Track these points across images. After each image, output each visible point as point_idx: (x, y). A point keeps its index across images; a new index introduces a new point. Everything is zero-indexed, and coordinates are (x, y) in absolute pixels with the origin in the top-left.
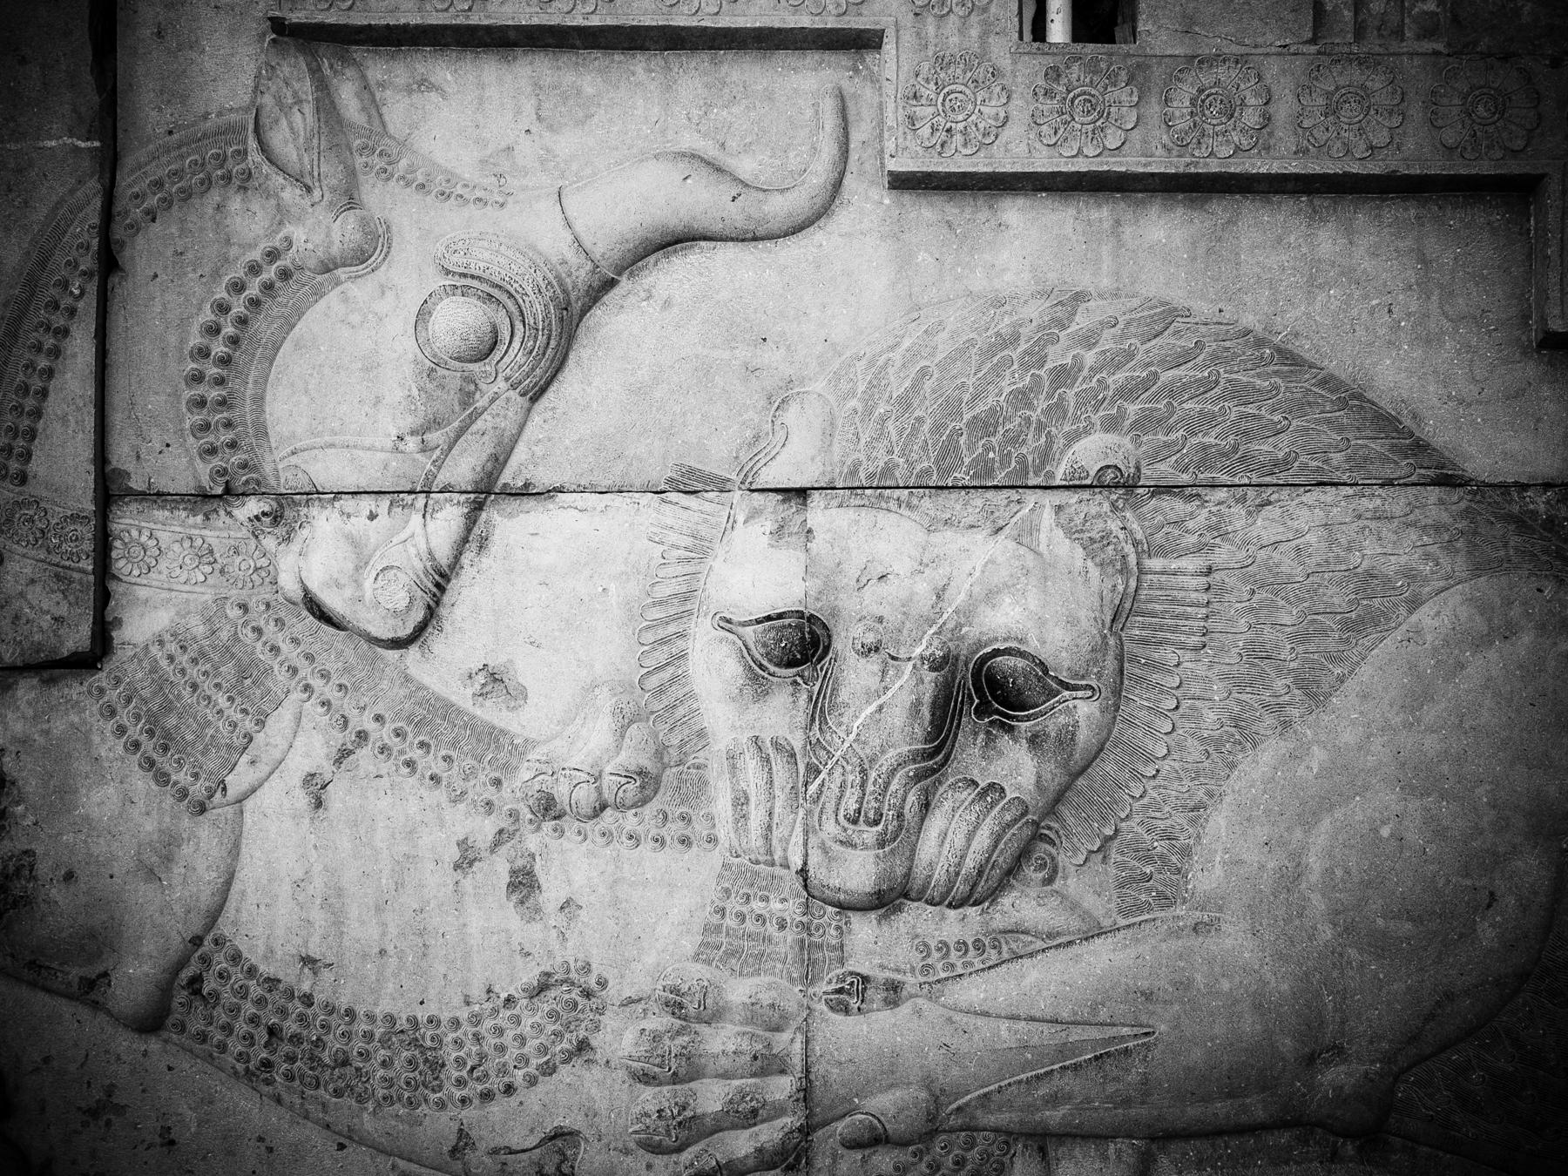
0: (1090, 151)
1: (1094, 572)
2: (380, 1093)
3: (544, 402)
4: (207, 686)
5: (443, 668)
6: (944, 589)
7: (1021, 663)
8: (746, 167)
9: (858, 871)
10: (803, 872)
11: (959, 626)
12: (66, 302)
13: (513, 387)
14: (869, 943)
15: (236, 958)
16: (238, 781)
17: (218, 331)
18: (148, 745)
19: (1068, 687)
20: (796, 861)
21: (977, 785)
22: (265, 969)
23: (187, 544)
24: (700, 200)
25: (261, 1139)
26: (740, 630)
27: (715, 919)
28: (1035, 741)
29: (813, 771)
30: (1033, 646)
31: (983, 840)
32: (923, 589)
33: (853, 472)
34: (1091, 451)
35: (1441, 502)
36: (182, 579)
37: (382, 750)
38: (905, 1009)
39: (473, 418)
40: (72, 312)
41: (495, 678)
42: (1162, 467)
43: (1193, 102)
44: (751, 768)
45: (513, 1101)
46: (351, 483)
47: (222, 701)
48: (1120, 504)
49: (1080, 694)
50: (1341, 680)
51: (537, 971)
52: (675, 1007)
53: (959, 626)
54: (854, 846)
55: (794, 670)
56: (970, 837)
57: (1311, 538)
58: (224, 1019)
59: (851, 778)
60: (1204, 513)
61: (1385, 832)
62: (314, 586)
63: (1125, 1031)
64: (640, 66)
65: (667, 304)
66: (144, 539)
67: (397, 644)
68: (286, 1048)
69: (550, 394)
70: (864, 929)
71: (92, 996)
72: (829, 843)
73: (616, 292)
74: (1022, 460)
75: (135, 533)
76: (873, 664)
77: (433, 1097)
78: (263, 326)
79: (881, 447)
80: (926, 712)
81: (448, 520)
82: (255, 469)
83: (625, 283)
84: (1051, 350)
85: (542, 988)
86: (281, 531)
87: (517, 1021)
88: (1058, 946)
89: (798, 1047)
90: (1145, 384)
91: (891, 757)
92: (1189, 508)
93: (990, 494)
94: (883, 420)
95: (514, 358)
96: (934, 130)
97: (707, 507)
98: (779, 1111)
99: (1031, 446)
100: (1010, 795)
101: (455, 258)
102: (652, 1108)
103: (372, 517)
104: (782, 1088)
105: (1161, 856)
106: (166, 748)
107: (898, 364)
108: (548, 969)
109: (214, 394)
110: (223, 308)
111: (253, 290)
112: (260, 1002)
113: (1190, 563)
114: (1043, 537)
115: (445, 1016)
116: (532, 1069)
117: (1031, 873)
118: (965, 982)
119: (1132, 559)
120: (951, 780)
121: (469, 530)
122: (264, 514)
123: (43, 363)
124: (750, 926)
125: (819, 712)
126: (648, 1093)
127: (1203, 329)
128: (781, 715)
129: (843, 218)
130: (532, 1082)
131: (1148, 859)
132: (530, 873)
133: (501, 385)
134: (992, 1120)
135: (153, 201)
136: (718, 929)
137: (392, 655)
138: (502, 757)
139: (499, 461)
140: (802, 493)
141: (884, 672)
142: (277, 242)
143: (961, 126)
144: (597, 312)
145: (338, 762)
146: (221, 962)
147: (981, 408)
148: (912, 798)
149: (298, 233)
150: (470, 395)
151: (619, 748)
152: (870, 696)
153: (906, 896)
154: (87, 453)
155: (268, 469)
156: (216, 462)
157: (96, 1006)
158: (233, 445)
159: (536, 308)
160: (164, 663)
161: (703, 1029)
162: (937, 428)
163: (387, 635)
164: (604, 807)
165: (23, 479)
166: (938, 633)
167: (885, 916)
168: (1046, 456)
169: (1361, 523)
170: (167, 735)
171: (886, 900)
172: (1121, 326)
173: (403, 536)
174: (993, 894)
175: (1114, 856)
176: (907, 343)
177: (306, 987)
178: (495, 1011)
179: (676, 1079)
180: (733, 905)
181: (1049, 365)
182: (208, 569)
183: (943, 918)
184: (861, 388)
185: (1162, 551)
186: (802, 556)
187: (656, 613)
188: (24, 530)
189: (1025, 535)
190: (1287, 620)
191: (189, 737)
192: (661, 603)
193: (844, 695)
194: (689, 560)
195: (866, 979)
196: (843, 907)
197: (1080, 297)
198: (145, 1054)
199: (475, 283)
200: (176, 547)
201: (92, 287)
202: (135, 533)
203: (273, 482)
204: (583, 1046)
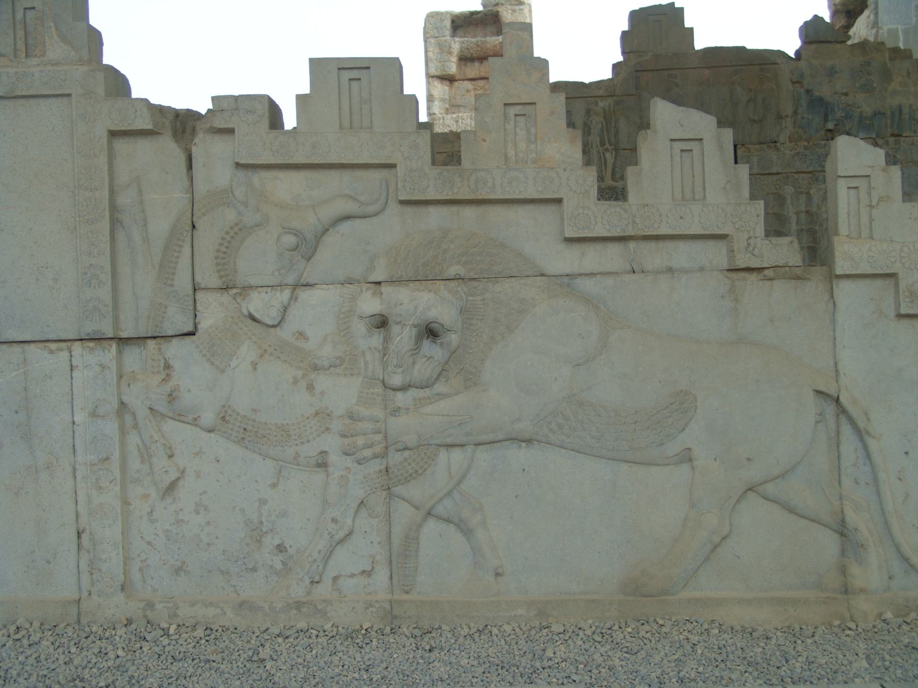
5: (286, 333)
8: (362, 198)
9: (397, 380)
10: (383, 381)
14: (400, 398)
15: (234, 411)
16: (233, 363)
20: (381, 378)
22: (242, 413)
24: (350, 207)
28: (441, 344)
29: (385, 355)
30: (440, 320)
40: (184, 241)
41: (301, 334)
46: (261, 284)
52: (351, 418)
62: (252, 311)
64: (334, 174)
65: (343, 235)
67: (274, 326)
70: (399, 395)
73: (329, 232)
80: (413, 339)
81: (287, 293)
83: (331, 230)
85: (317, 414)
104: (379, 437)
110: (223, 239)
113: (479, 298)
117: (442, 379)
123: (176, 254)
125: (387, 340)
126: (345, 440)
128: (376, 340)
134: (433, 442)
137: (272, 330)
140: (379, 283)
144: (324, 237)
146: (230, 412)
154: (190, 278)
156: (224, 279)
157: (196, 425)
165: (172, 286)
171: (403, 388)
174: (433, 384)
179: (352, 436)
187: (343, 316)
201: (189, 234)
204: (327, 429)
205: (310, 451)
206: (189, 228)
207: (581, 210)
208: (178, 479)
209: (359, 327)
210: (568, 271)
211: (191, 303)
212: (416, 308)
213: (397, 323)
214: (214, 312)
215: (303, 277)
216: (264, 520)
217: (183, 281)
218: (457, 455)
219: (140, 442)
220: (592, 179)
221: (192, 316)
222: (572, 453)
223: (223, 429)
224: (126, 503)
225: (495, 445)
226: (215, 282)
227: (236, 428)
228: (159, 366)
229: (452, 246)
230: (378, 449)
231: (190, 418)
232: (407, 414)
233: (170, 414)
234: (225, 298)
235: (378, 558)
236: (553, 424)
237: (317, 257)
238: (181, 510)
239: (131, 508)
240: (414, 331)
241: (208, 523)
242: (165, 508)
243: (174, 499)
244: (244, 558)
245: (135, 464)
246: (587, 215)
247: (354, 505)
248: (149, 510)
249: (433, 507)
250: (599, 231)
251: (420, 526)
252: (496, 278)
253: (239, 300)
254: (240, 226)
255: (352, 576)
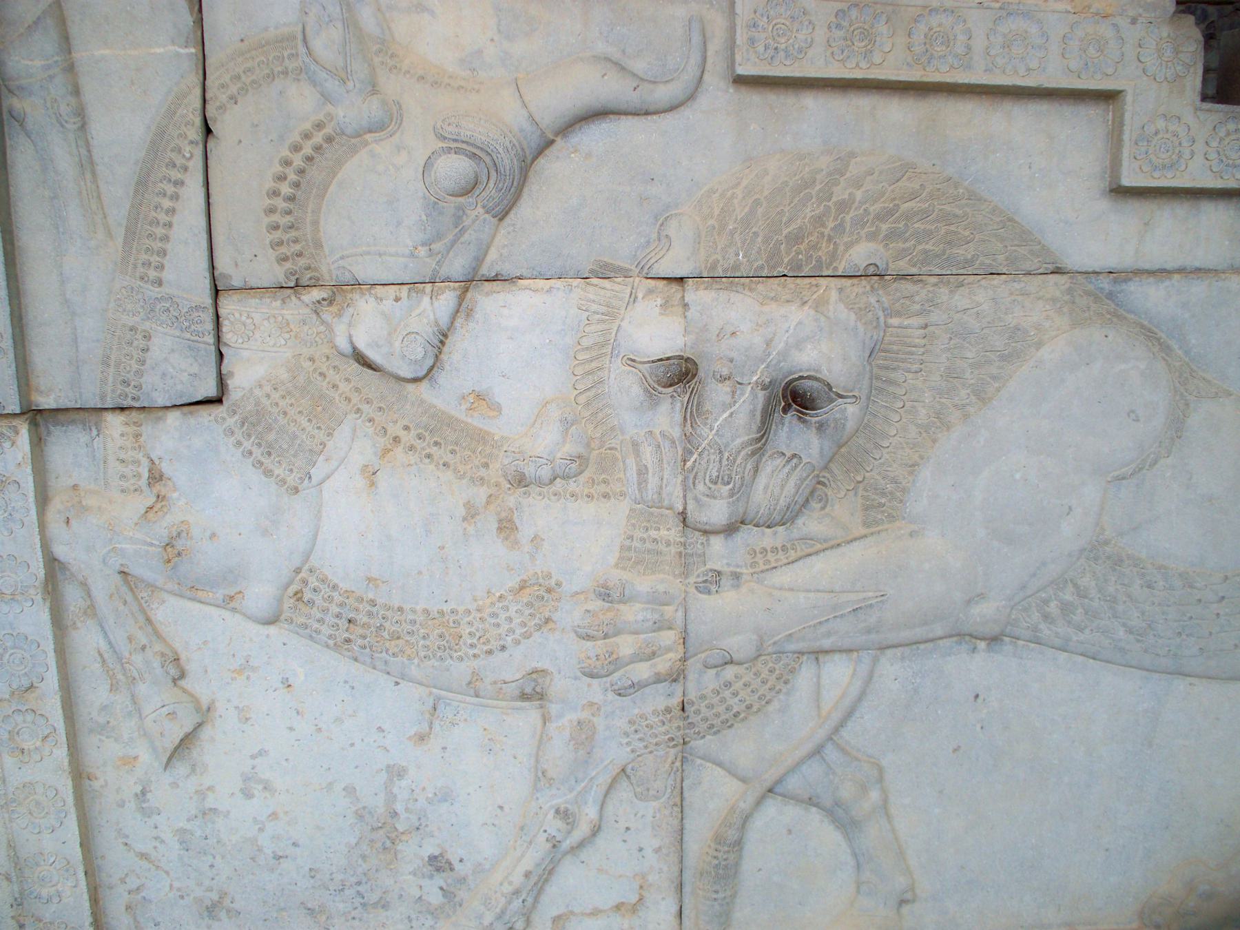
0: (863, 65)
1: (861, 329)
2: (422, 654)
3: (507, 220)
4: (292, 412)
6: (771, 340)
7: (815, 384)
8: (639, 66)
9: (717, 512)
11: (779, 362)
12: (179, 161)
13: (487, 212)
14: (719, 552)
15: (323, 581)
16: (317, 473)
17: (285, 178)
18: (257, 452)
19: (841, 396)
21: (784, 454)
22: (343, 586)
23: (272, 320)
24: (612, 89)
25: (346, 682)
26: (640, 366)
27: (628, 543)
28: (821, 427)
30: (825, 374)
31: (790, 487)
32: (758, 340)
33: (714, 266)
34: (861, 254)
35: (1056, 284)
36: (271, 343)
37: (412, 448)
38: (744, 589)
39: (463, 231)
40: (186, 169)
41: (480, 397)
42: (901, 263)
43: (926, 36)
44: (648, 453)
45: (506, 654)
47: (305, 423)
48: (876, 285)
49: (849, 400)
50: (998, 390)
51: (518, 579)
53: (779, 362)
54: (715, 498)
55: (671, 389)
56: (783, 487)
57: (985, 307)
58: (319, 615)
59: (712, 457)
60: (924, 292)
61: (1018, 476)
62: (362, 346)
63: (871, 594)
66: (244, 318)
67: (416, 380)
68: (360, 631)
69: (512, 215)
70: (717, 543)
71: (232, 605)
72: (700, 497)
74: (819, 260)
75: (237, 315)
76: (726, 388)
77: (455, 655)
78: (314, 173)
79: (732, 251)
81: (447, 300)
82: (316, 270)
83: (560, 142)
84: (835, 189)
85: (522, 588)
86: (334, 309)
87: (506, 609)
88: (832, 547)
89: (680, 614)
90: (890, 213)
91: (738, 441)
92: (916, 288)
93: (798, 281)
94: (732, 234)
95: (490, 191)
96: (766, 48)
97: (617, 287)
98: (669, 650)
99: (825, 249)
100: (804, 461)
101: (450, 129)
102: (592, 654)
103: (397, 299)
104: (669, 637)
105: (891, 493)
106: (269, 454)
107: (740, 196)
108: (525, 578)
109: (284, 221)
110: (287, 163)
111: (307, 150)
112: (341, 605)
114: (831, 308)
115: (461, 609)
116: (517, 636)
117: (815, 505)
118: (778, 572)
119: (882, 320)
120: (770, 453)
121: (460, 305)
122: (324, 299)
123: (167, 203)
124: (648, 545)
126: (589, 644)
127: (924, 176)
128: (666, 416)
129: (703, 101)
130: (517, 642)
131: (883, 494)
132: (511, 521)
133: (481, 211)
134: (792, 647)
135: (233, 89)
136: (629, 548)
137: (411, 387)
138: (488, 450)
139: (479, 260)
140: (681, 280)
141: (734, 393)
142: (321, 117)
143: (783, 46)
144: (541, 161)
145: (383, 456)
146: (313, 582)
147: (793, 226)
148: (749, 466)
149: (340, 112)
150: (460, 218)
151: (564, 442)
152: (725, 406)
153: (742, 522)
154: (204, 264)
155: (324, 269)
156: (288, 265)
157: (234, 610)
158: (300, 255)
159: (507, 162)
160: (264, 401)
161: (622, 607)
162: (766, 240)
163: (410, 376)
164: (555, 479)
165: (160, 283)
166: (767, 367)
167: (730, 535)
168: (833, 256)
169: (1013, 298)
170: (270, 446)
172: (876, 174)
173: (418, 312)
174: (793, 520)
175: (861, 492)
176: (745, 183)
177: (371, 595)
178: (493, 604)
179: (606, 636)
180: (639, 534)
181: (834, 199)
182: (287, 336)
183: (763, 534)
184: (717, 212)
185: (898, 314)
186: (682, 320)
188: (164, 317)
189: (819, 305)
190: (969, 355)
191: (285, 446)
192: (587, 348)
193: (707, 406)
194: (604, 321)
195: (719, 573)
196: (706, 532)
197: (852, 155)
198: (268, 636)
199: (464, 146)
200: (266, 322)
201: (198, 152)
202: (237, 315)
203: (327, 277)
205: (511, 667)
206: (195, 133)
207: (1161, 124)
208: (200, 725)
209: (625, 387)
210: (1112, 262)
211: (209, 326)
212: (768, 343)
213: (723, 379)
214: (265, 346)
215: (489, 259)
216: (399, 807)
217: (186, 273)
218: (839, 674)
219: (103, 645)
220: (1192, 49)
221: (213, 358)
222: (1081, 658)
223: (302, 620)
224: (79, 774)
225: (922, 646)
226: (267, 270)
227: (330, 619)
228: (138, 476)
229: (859, 195)
230: (663, 664)
231: (220, 594)
232: (737, 587)
233: (169, 586)
234: (295, 309)
235: (651, 878)
236: (1053, 604)
237: (525, 210)
238: (210, 788)
239: (96, 785)
240: (761, 395)
241: (274, 816)
242: (175, 785)
243: (193, 768)
244: (359, 883)
245: (95, 694)
246: (1176, 135)
247: (604, 780)
248: (139, 789)
249: (779, 781)
250: (1196, 175)
251: (746, 819)
252: (957, 274)
253: (327, 317)
254: (328, 130)
255: (595, 913)
